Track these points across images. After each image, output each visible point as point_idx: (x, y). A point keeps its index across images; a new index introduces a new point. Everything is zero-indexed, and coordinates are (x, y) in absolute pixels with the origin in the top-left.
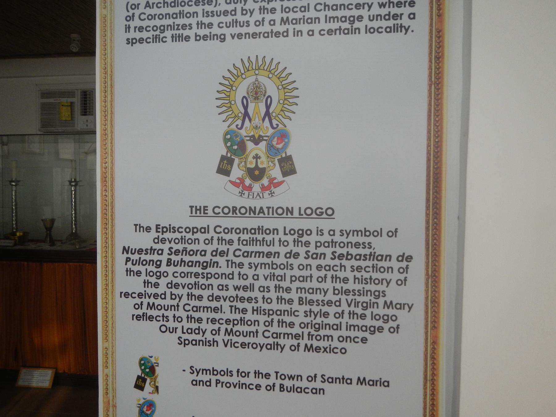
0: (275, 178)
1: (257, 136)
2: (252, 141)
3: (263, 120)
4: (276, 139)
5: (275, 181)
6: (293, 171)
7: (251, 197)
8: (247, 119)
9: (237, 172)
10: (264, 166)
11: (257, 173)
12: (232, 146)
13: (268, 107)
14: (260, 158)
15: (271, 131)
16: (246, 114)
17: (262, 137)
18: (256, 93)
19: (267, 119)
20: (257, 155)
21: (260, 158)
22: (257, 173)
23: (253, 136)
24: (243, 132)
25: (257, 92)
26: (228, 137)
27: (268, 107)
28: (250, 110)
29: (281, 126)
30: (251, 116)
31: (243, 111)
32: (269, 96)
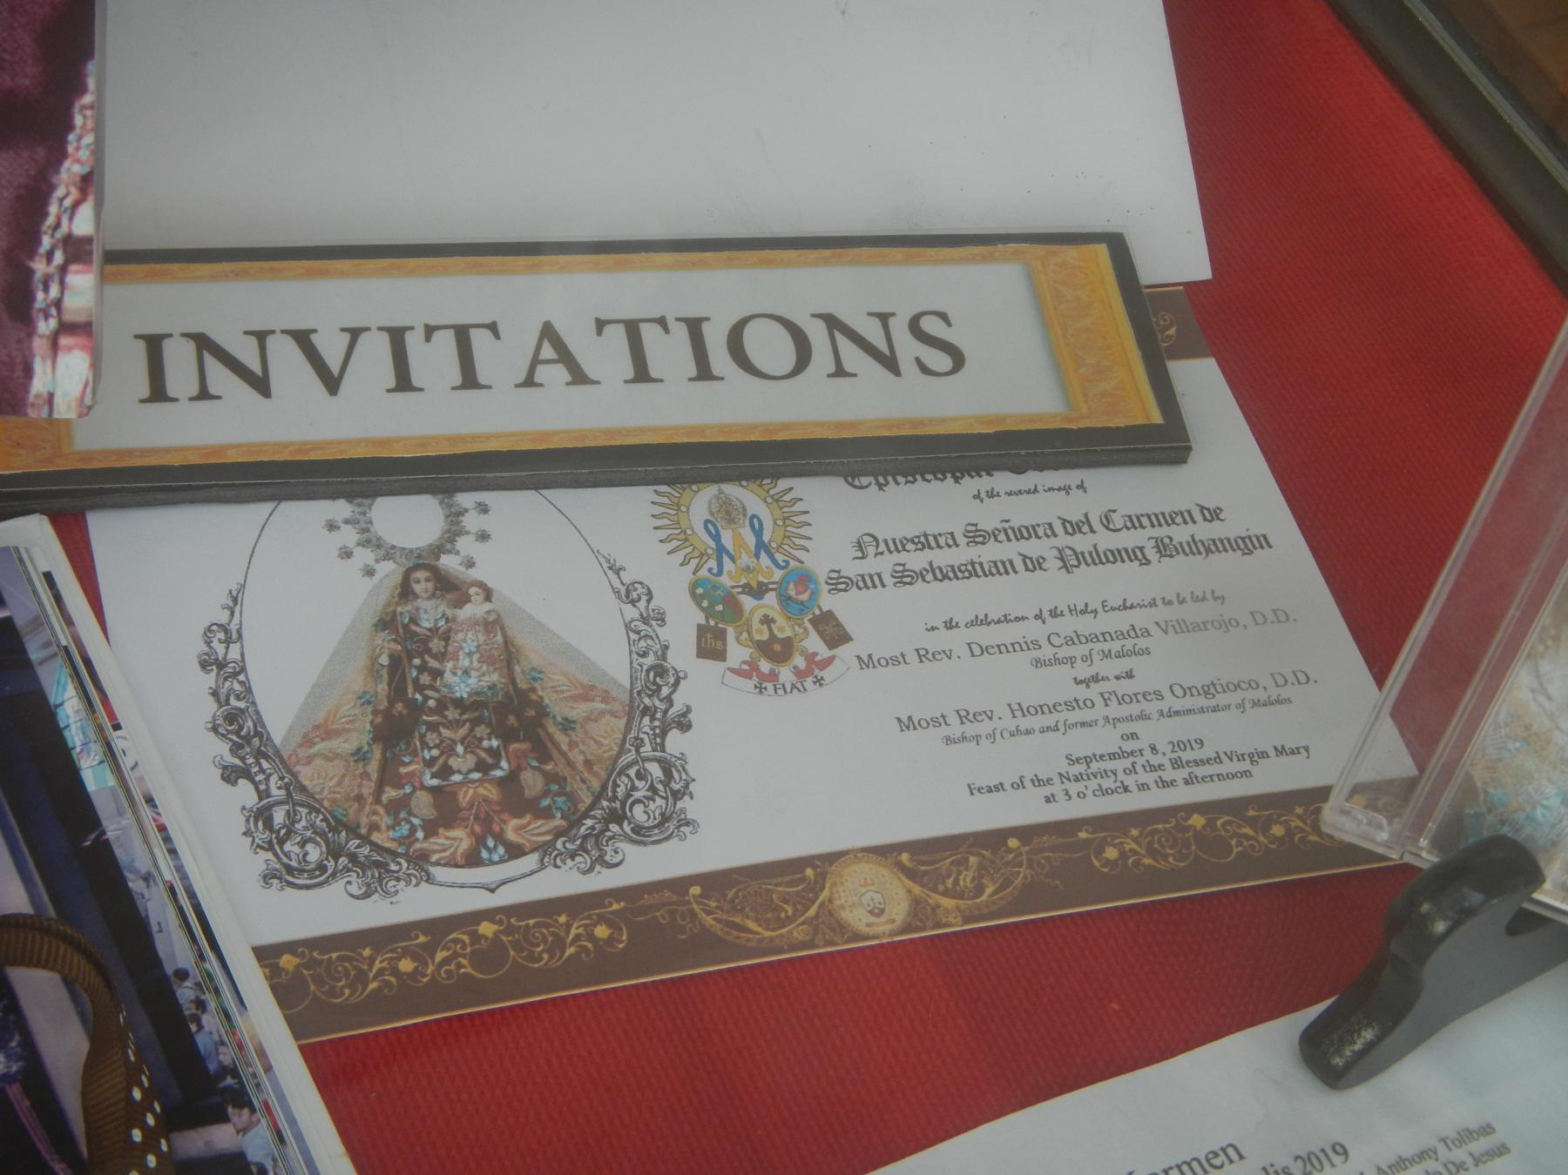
0: (815, 654)
1: (754, 585)
2: (749, 594)
3: (757, 556)
4: (792, 586)
5: (818, 658)
7: (781, 692)
8: (726, 559)
9: (738, 654)
10: (788, 633)
11: (777, 647)
12: (711, 605)
13: (758, 533)
15: (778, 575)
16: (721, 550)
17: (766, 584)
18: (728, 513)
19: (763, 555)
20: (765, 616)
21: (773, 621)
23: (747, 585)
26: (700, 591)
27: (758, 533)
29: (793, 564)
31: (713, 545)
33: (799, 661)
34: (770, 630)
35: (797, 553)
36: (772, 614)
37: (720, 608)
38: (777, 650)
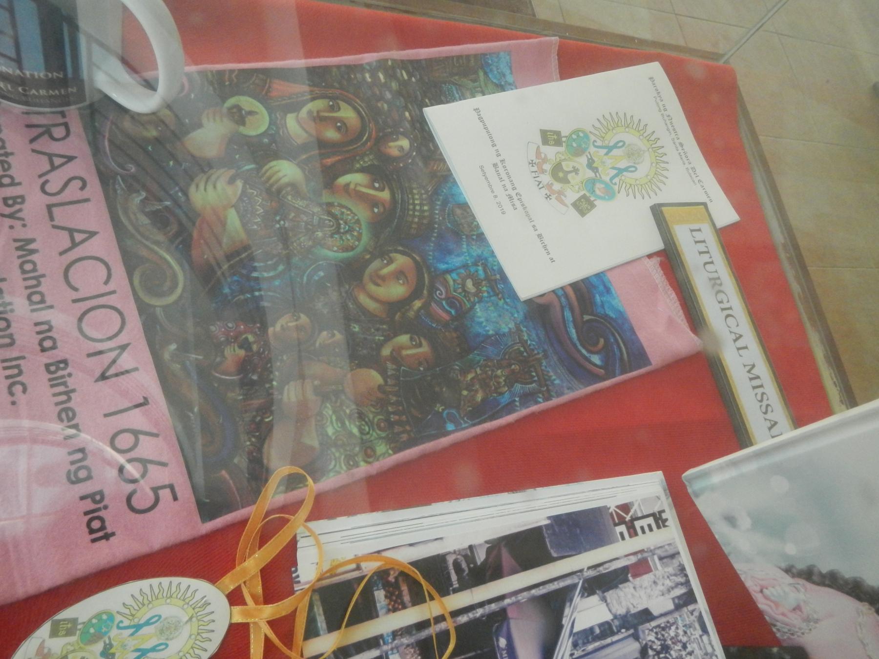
1: (595, 165)
5: (563, 197)
6: (583, 213)
9: (551, 152)
12: (574, 140)
14: (577, 174)
15: (607, 179)
16: (610, 149)
17: (597, 171)
19: (615, 172)
21: (577, 174)
22: (561, 175)
23: (594, 161)
24: (592, 149)
25: (633, 154)
26: (581, 135)
27: (626, 169)
28: (615, 152)
29: (616, 188)
30: (610, 154)
31: (611, 144)
32: (636, 169)
33: (557, 186)
34: (570, 172)
35: (623, 189)
36: (581, 172)
37: (575, 145)
38: (558, 172)
